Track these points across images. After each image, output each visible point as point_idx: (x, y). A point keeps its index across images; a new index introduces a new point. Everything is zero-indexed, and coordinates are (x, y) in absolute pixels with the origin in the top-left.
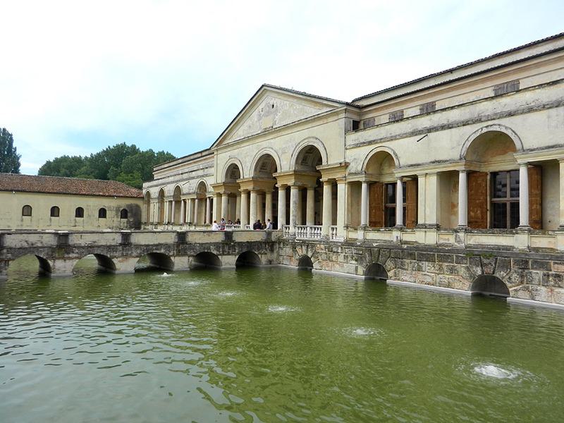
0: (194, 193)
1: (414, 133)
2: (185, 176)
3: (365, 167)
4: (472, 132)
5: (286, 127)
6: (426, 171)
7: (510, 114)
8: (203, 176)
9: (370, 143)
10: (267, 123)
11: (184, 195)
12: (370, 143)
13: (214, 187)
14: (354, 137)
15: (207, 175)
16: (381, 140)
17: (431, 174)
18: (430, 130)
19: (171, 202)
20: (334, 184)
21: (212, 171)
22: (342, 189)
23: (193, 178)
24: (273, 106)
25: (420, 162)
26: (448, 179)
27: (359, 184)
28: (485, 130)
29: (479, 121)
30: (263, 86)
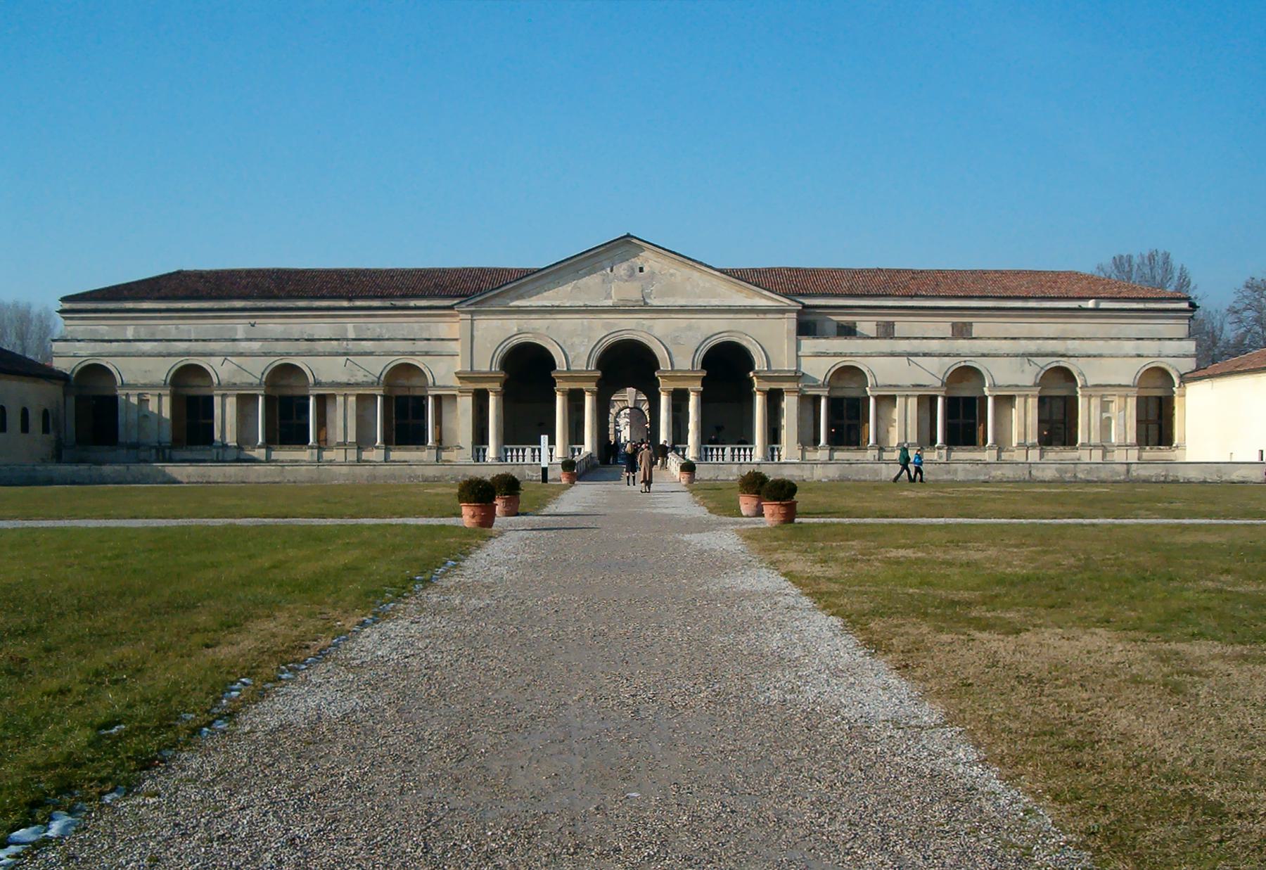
0: (371, 384)
1: (892, 355)
2: (320, 346)
3: (827, 380)
4: (951, 363)
5: (683, 310)
6: (909, 393)
7: (984, 355)
8: (413, 354)
9: (835, 355)
10: (632, 292)
11: (318, 384)
12: (835, 355)
13: (462, 377)
14: (808, 344)
15: (427, 354)
16: (851, 355)
17: (911, 396)
18: (909, 355)
19: (246, 401)
20: (774, 398)
21: (455, 347)
22: (789, 405)
23: (371, 354)
24: (641, 270)
25: (899, 384)
26: (927, 403)
27: (817, 399)
28: (963, 364)
29: (958, 355)
30: (628, 236)
